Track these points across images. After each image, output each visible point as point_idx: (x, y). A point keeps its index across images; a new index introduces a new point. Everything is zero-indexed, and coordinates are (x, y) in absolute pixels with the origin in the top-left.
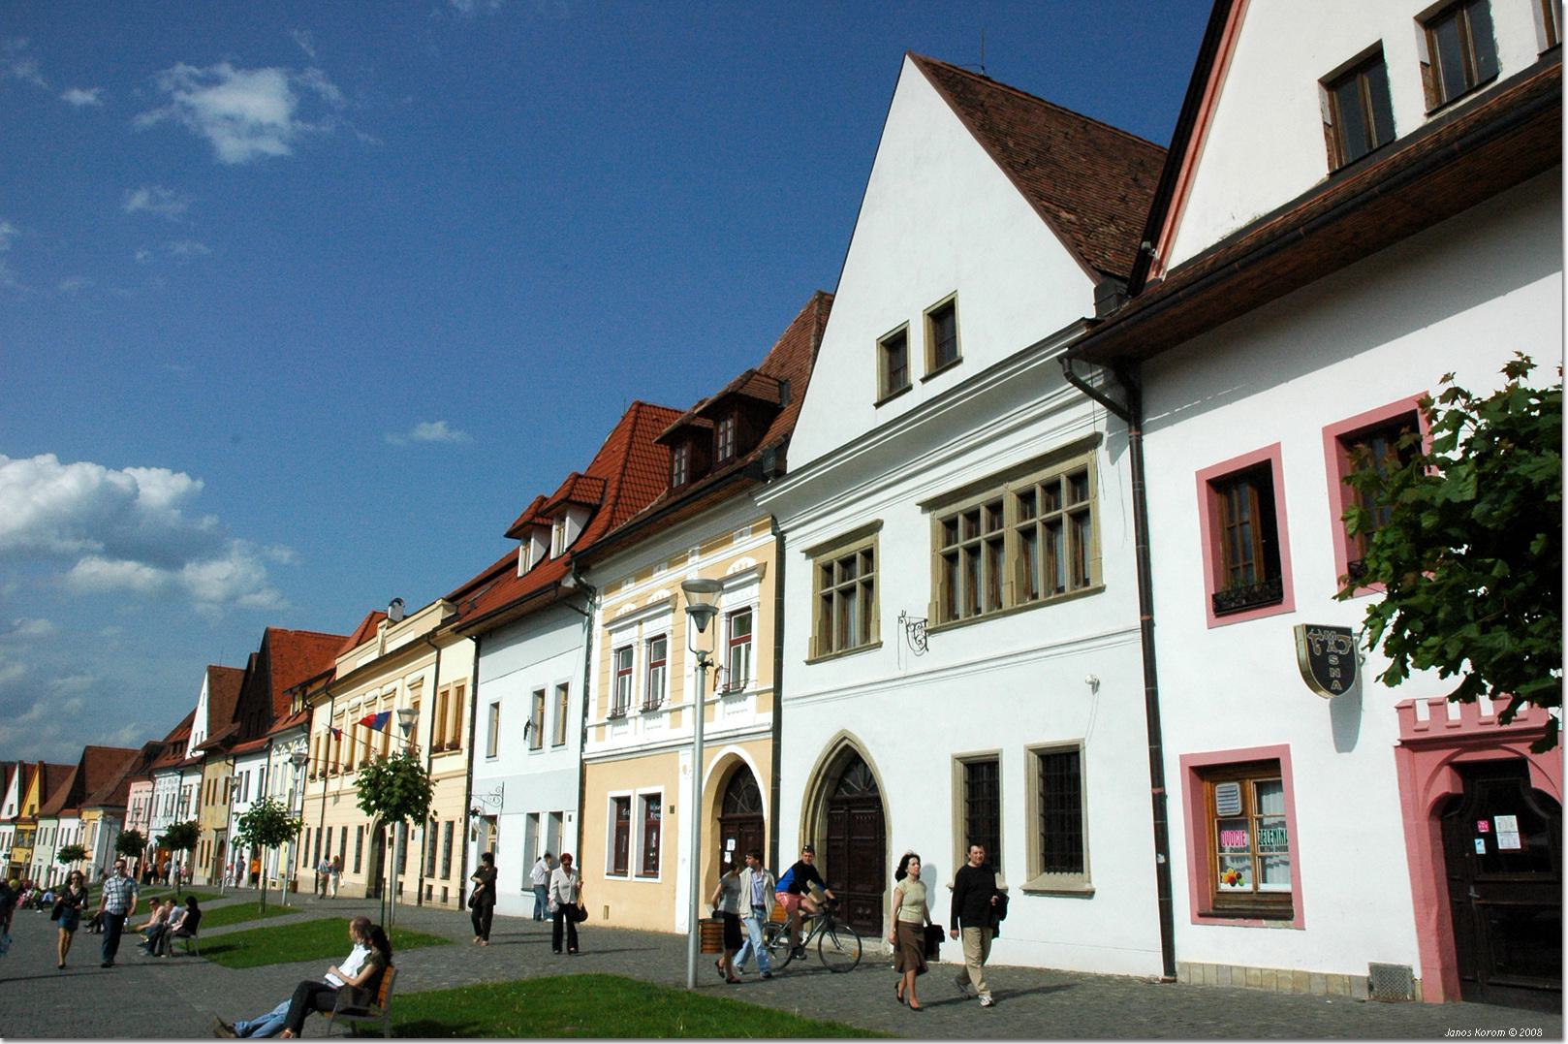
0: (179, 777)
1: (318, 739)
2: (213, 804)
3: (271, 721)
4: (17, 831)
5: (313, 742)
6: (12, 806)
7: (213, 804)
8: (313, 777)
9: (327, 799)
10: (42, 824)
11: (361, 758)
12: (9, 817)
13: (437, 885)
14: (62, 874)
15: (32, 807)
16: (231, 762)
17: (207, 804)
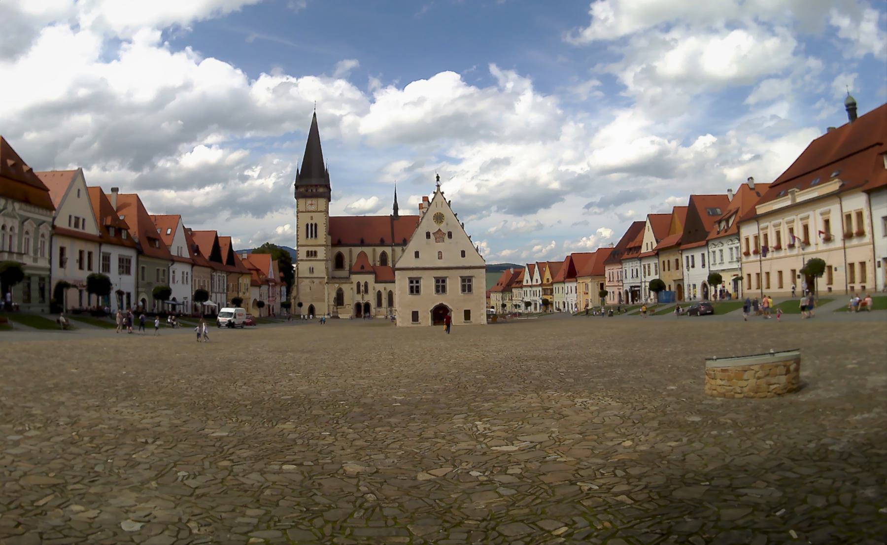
0: (639, 262)
1: (747, 239)
2: (669, 270)
3: (707, 233)
4: (543, 289)
5: (743, 241)
6: (537, 280)
7: (669, 270)
8: (747, 254)
9: (762, 262)
10: (555, 286)
11: (787, 243)
12: (538, 284)
13: (857, 286)
14: (572, 304)
15: (548, 279)
16: (680, 252)
17: (664, 270)
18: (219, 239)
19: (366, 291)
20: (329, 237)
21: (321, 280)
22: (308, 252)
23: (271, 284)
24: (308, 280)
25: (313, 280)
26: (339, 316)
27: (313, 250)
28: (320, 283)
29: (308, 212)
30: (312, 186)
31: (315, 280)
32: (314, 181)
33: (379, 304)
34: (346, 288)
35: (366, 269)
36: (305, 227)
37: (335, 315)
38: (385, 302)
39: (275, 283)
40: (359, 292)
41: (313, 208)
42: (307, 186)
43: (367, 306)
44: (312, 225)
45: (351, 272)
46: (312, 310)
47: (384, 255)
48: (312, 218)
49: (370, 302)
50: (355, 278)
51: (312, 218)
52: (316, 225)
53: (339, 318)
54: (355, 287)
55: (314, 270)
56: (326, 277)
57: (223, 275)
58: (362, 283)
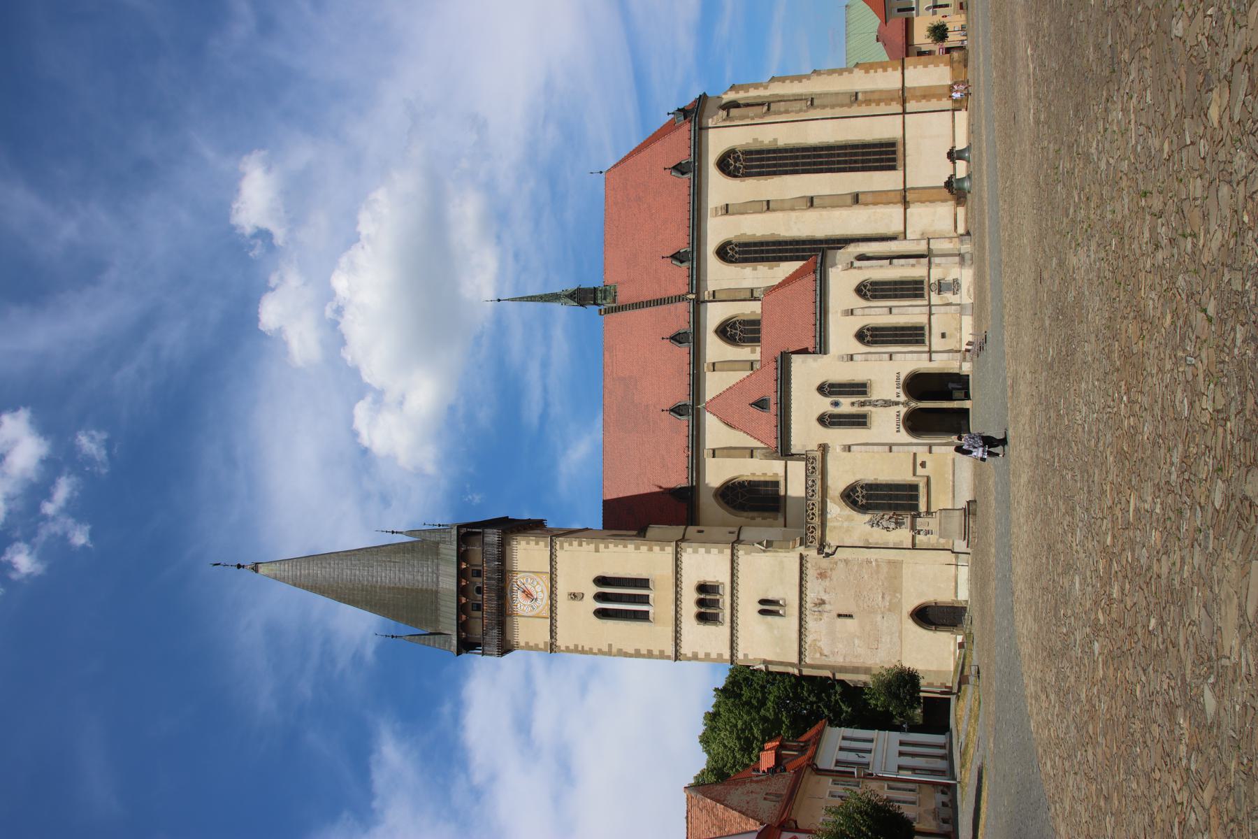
19: (858, 389)
20: (654, 531)
21: (811, 573)
22: (702, 618)
24: (811, 624)
25: (809, 605)
27: (695, 596)
28: (822, 575)
30: (461, 591)
31: (811, 596)
33: (912, 335)
34: (840, 476)
35: (769, 390)
38: (906, 313)
40: (859, 421)
41: (540, 589)
42: (461, 609)
43: (918, 385)
44: (600, 597)
45: (784, 451)
46: (927, 616)
47: (728, 332)
48: (574, 596)
49: (902, 378)
50: (804, 433)
51: (574, 596)
52: (601, 581)
54: (837, 437)
55: (770, 597)
56: (801, 549)
58: (824, 405)
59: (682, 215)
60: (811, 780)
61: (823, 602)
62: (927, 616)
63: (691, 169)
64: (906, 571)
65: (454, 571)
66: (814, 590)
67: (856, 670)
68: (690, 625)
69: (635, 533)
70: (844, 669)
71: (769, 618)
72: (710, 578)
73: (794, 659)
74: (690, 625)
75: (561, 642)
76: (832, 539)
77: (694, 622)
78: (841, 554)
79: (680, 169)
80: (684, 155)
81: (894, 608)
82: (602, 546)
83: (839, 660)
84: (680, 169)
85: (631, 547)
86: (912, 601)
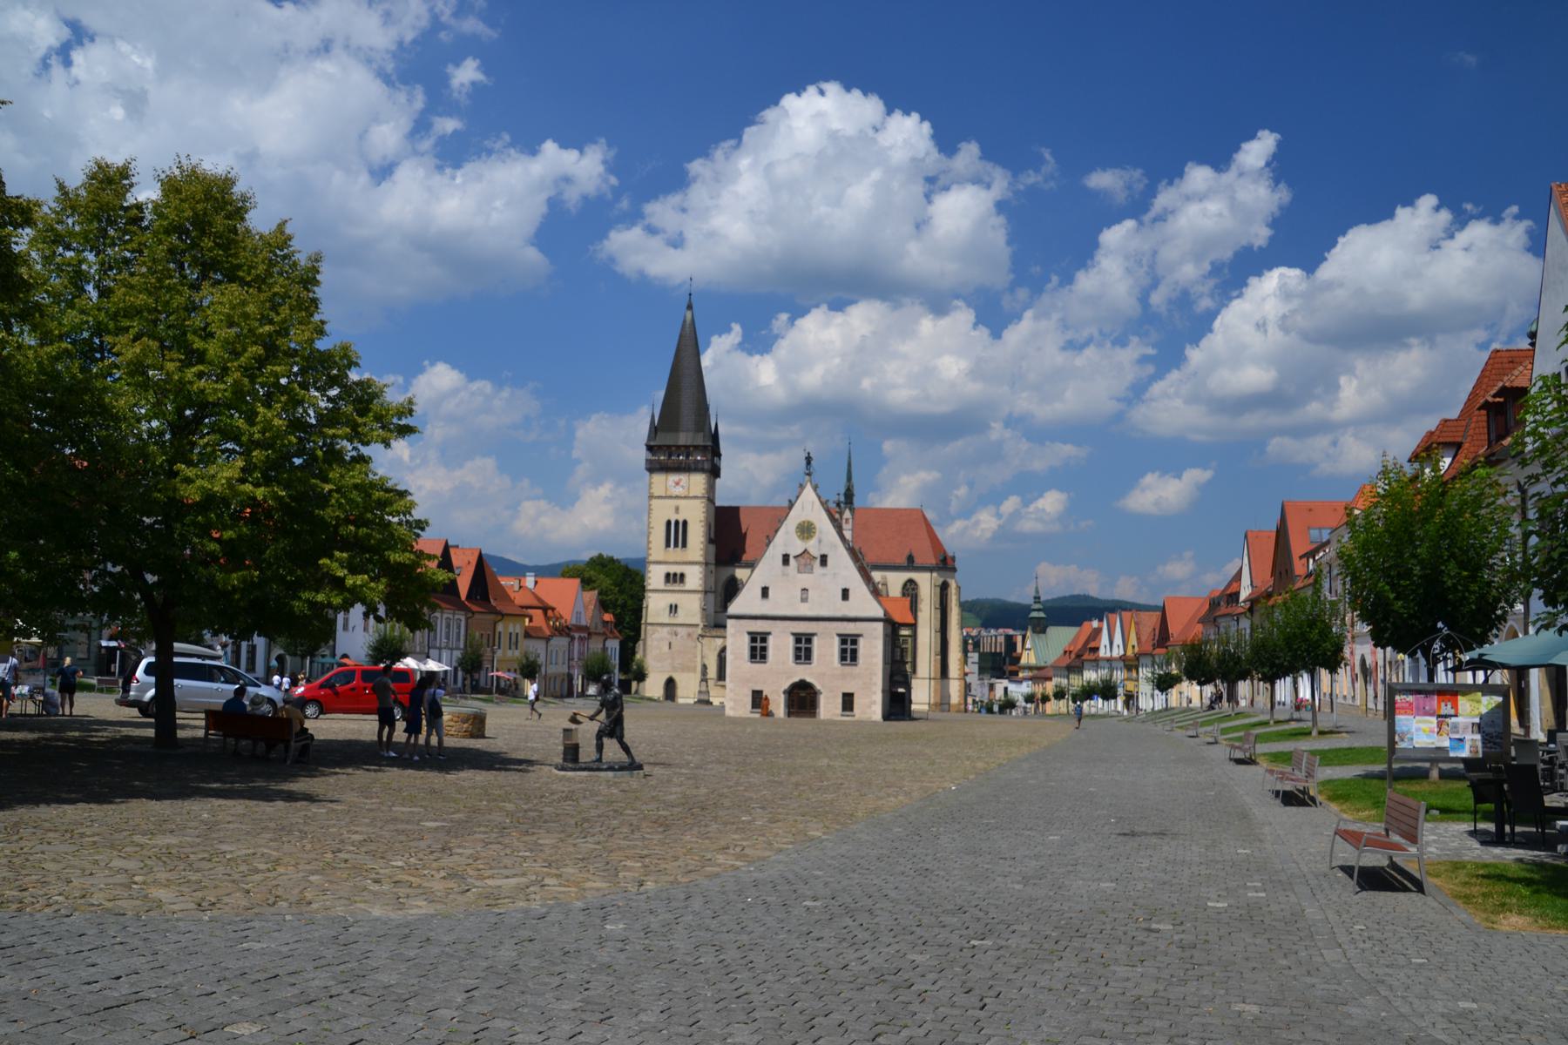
18: (452, 551)
20: (712, 548)
21: (690, 630)
22: (668, 575)
23: (577, 635)
24: (666, 629)
25: (675, 628)
26: (711, 700)
28: (689, 635)
29: (671, 497)
30: (678, 447)
31: (679, 629)
32: (683, 439)
36: (663, 528)
37: (704, 697)
39: (590, 634)
41: (678, 491)
42: (669, 447)
44: (677, 523)
46: (670, 685)
48: (677, 509)
51: (677, 509)
52: (685, 523)
53: (711, 703)
55: (679, 610)
56: (701, 625)
57: (457, 617)
59: (884, 560)
60: (601, 639)
61: (676, 635)
62: (670, 685)
63: (911, 564)
64: (692, 675)
65: (688, 444)
66: (682, 631)
67: (644, 650)
68: (663, 569)
69: (712, 536)
70: (645, 644)
71: (668, 609)
72: (687, 579)
73: (649, 621)
74: (663, 569)
75: (654, 502)
76: (705, 641)
77: (666, 571)
78: (699, 644)
79: (910, 559)
80: (918, 561)
81: (674, 669)
82: (703, 524)
83: (649, 642)
84: (910, 559)
85: (702, 539)
86: (677, 677)
